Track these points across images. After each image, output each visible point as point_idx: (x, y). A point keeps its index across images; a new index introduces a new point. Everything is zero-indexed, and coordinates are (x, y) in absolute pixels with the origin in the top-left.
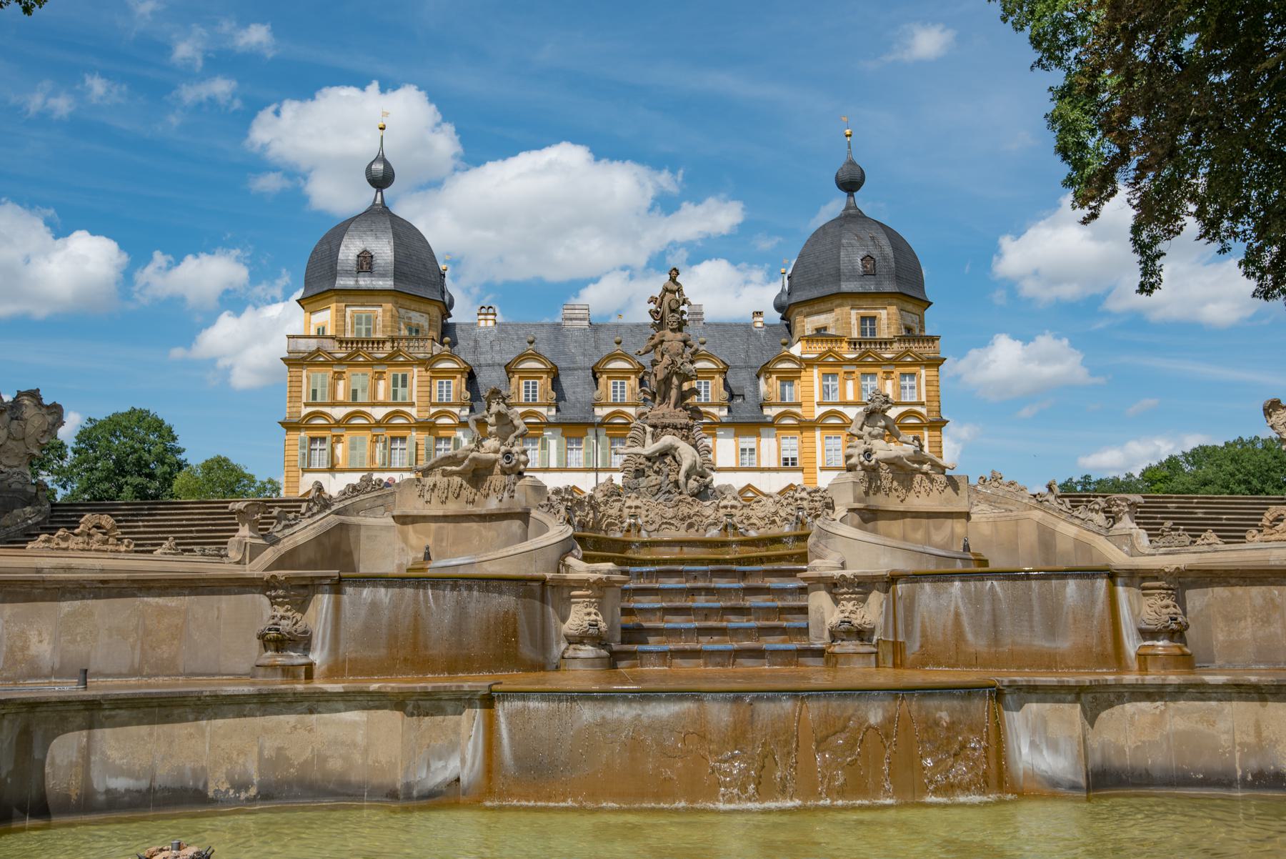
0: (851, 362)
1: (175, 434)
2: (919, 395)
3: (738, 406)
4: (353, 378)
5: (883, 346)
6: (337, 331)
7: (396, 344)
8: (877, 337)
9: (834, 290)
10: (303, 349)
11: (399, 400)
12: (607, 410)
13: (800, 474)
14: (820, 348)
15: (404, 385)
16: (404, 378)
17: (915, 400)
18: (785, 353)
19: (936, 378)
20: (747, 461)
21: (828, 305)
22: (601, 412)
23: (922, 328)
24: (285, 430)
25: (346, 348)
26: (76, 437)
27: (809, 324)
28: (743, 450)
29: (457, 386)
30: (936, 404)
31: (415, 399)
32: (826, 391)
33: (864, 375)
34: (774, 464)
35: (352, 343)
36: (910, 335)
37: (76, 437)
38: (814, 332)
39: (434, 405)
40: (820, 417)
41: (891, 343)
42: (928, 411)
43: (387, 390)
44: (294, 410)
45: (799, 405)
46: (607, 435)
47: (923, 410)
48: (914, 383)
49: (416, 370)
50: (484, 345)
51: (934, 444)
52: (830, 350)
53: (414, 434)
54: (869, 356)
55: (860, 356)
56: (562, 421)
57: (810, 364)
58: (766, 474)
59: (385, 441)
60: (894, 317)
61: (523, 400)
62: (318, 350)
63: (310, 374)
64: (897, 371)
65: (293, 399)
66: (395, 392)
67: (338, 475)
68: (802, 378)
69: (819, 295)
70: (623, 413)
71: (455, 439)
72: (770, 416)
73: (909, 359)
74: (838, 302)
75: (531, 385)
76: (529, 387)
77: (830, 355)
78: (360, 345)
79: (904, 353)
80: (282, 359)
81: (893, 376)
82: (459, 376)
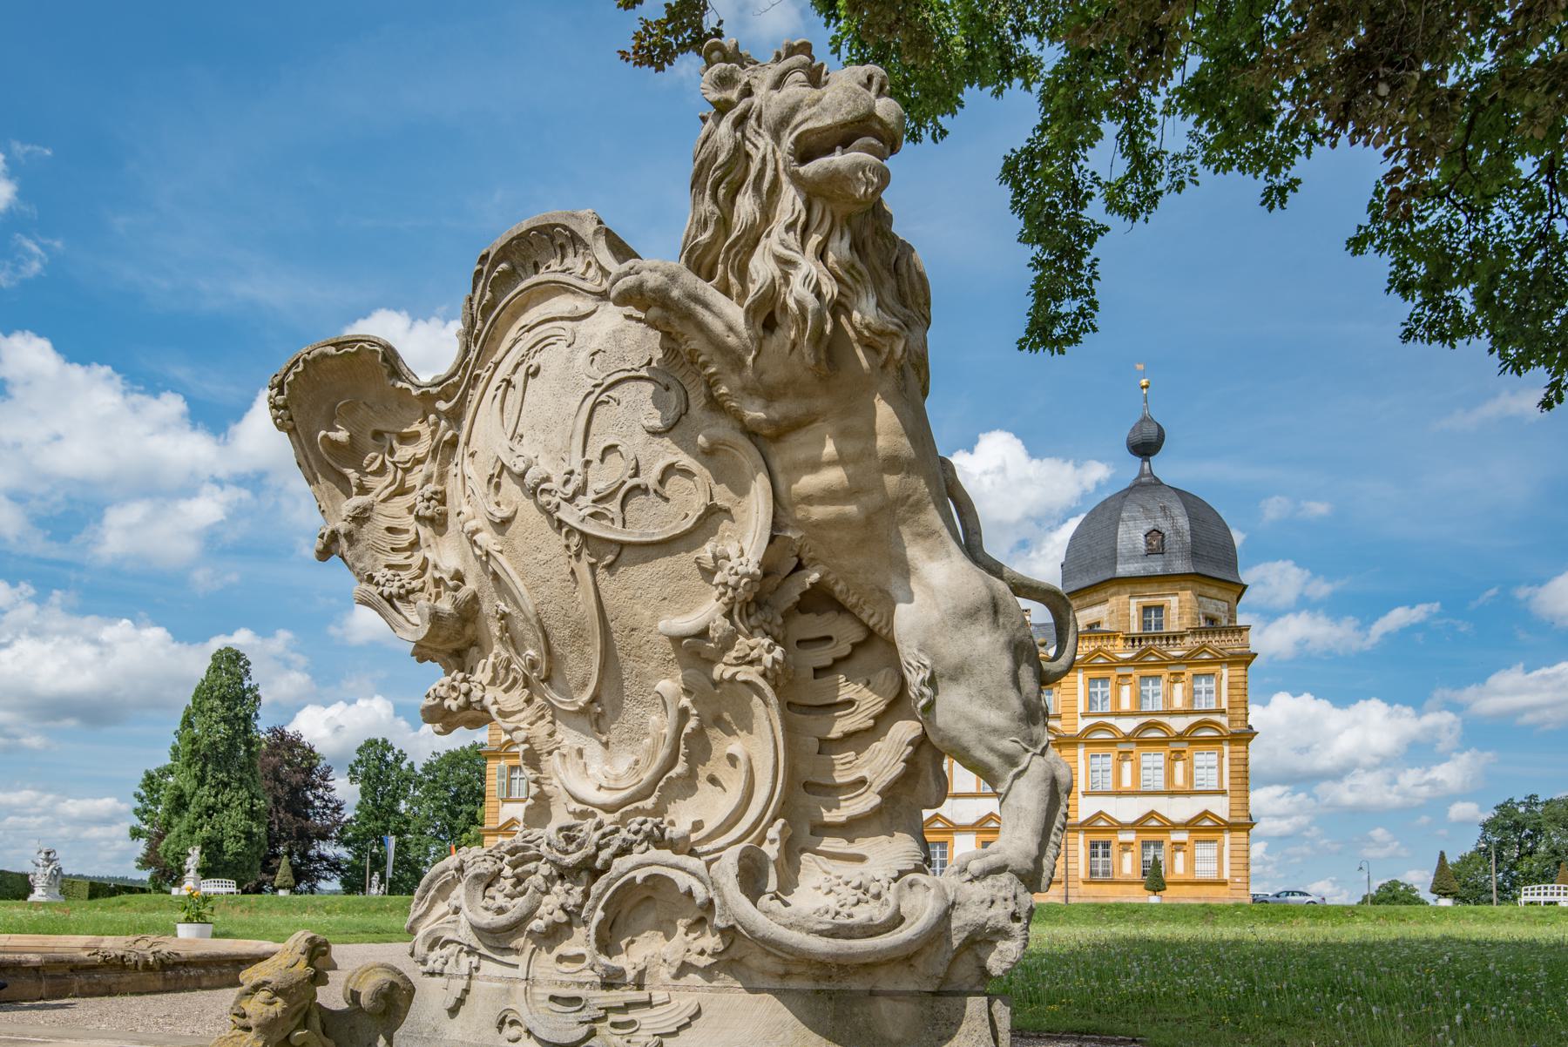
0: (1126, 663)
5: (1171, 642)
9: (1108, 575)
17: (1213, 707)
19: (1242, 679)
21: (1102, 595)
23: (1232, 616)
27: (1084, 617)
30: (1243, 711)
32: (1091, 699)
36: (1212, 625)
40: (1083, 732)
41: (1182, 637)
42: (1231, 721)
47: (1224, 720)
48: (1213, 686)
51: (1236, 762)
52: (1099, 650)
54: (1151, 654)
55: (1138, 655)
60: (1188, 605)
73: (1206, 656)
74: (1113, 590)
81: (1184, 678)
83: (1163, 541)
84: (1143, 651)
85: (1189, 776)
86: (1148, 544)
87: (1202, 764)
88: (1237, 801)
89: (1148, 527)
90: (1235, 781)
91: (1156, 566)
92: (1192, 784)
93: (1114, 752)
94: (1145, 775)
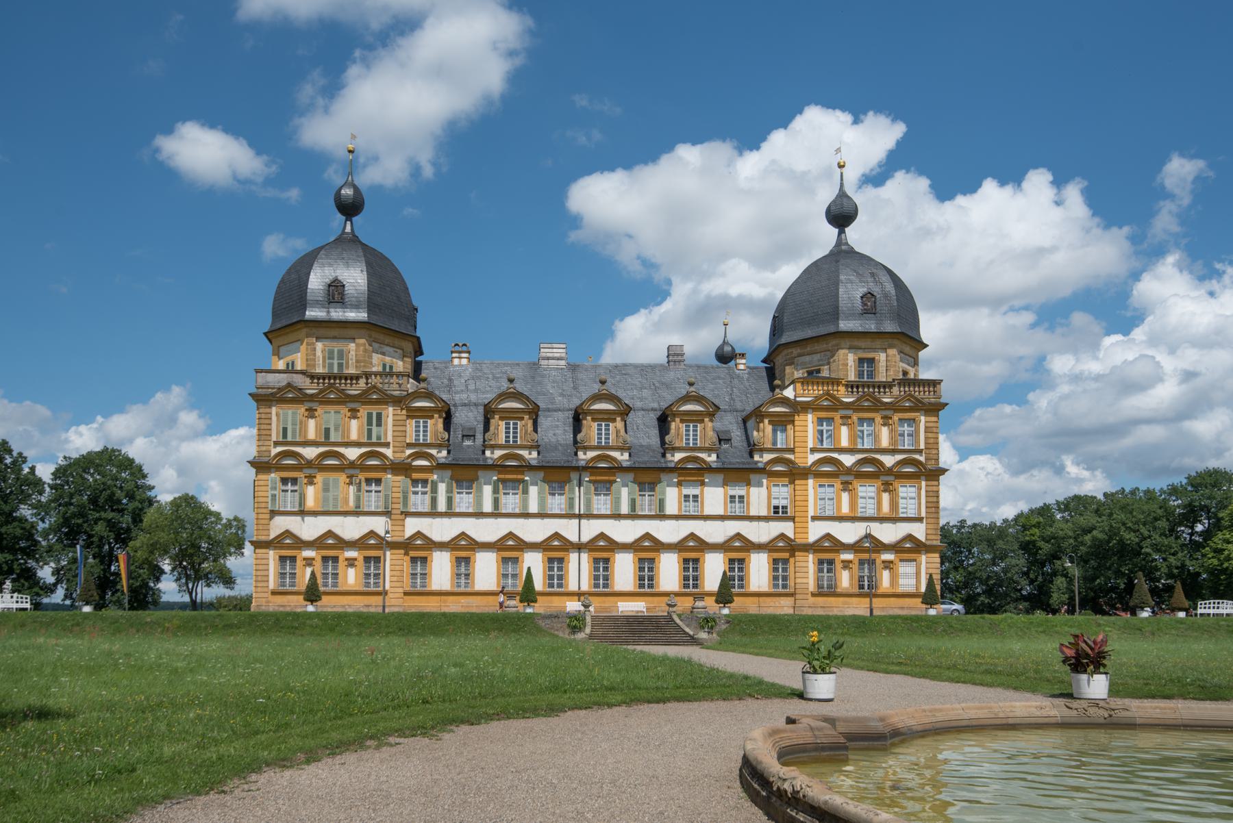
0: (847, 406)
1: (145, 471)
2: (918, 442)
3: (726, 451)
4: (325, 416)
5: (882, 390)
6: (308, 365)
7: (370, 381)
8: (876, 380)
9: (832, 329)
10: (271, 385)
11: (374, 440)
12: (591, 454)
13: (791, 524)
14: (817, 391)
15: (379, 424)
16: (379, 416)
18: (780, 396)
20: (737, 510)
22: (584, 457)
24: (254, 470)
25: (318, 383)
26: (52, 474)
28: (732, 497)
29: (435, 425)
31: (390, 439)
33: (861, 420)
34: (764, 513)
35: (324, 379)
37: (52, 474)
38: (806, 375)
39: (409, 445)
40: (814, 463)
42: (926, 459)
43: (360, 429)
44: (264, 448)
45: (792, 451)
46: (590, 481)
47: (922, 458)
49: (391, 409)
50: (459, 383)
51: (931, 494)
53: (389, 476)
54: (867, 400)
55: (858, 400)
56: (544, 464)
57: (805, 408)
58: (755, 523)
59: (360, 483)
61: (502, 439)
62: (289, 385)
63: (281, 412)
64: (896, 417)
65: (263, 438)
66: (370, 431)
67: (307, 519)
68: (796, 423)
69: (814, 335)
70: (609, 456)
71: (432, 481)
72: (761, 462)
75: (511, 426)
76: (509, 428)
77: (826, 399)
78: (332, 381)
79: (904, 398)
80: (250, 394)
82: (436, 416)
83: (875, 303)
84: (862, 397)
85: (894, 505)
86: (864, 304)
87: (905, 495)
88: (931, 526)
89: (863, 290)
90: (930, 510)
91: (871, 326)
92: (897, 512)
93: (838, 484)
94: (861, 502)
